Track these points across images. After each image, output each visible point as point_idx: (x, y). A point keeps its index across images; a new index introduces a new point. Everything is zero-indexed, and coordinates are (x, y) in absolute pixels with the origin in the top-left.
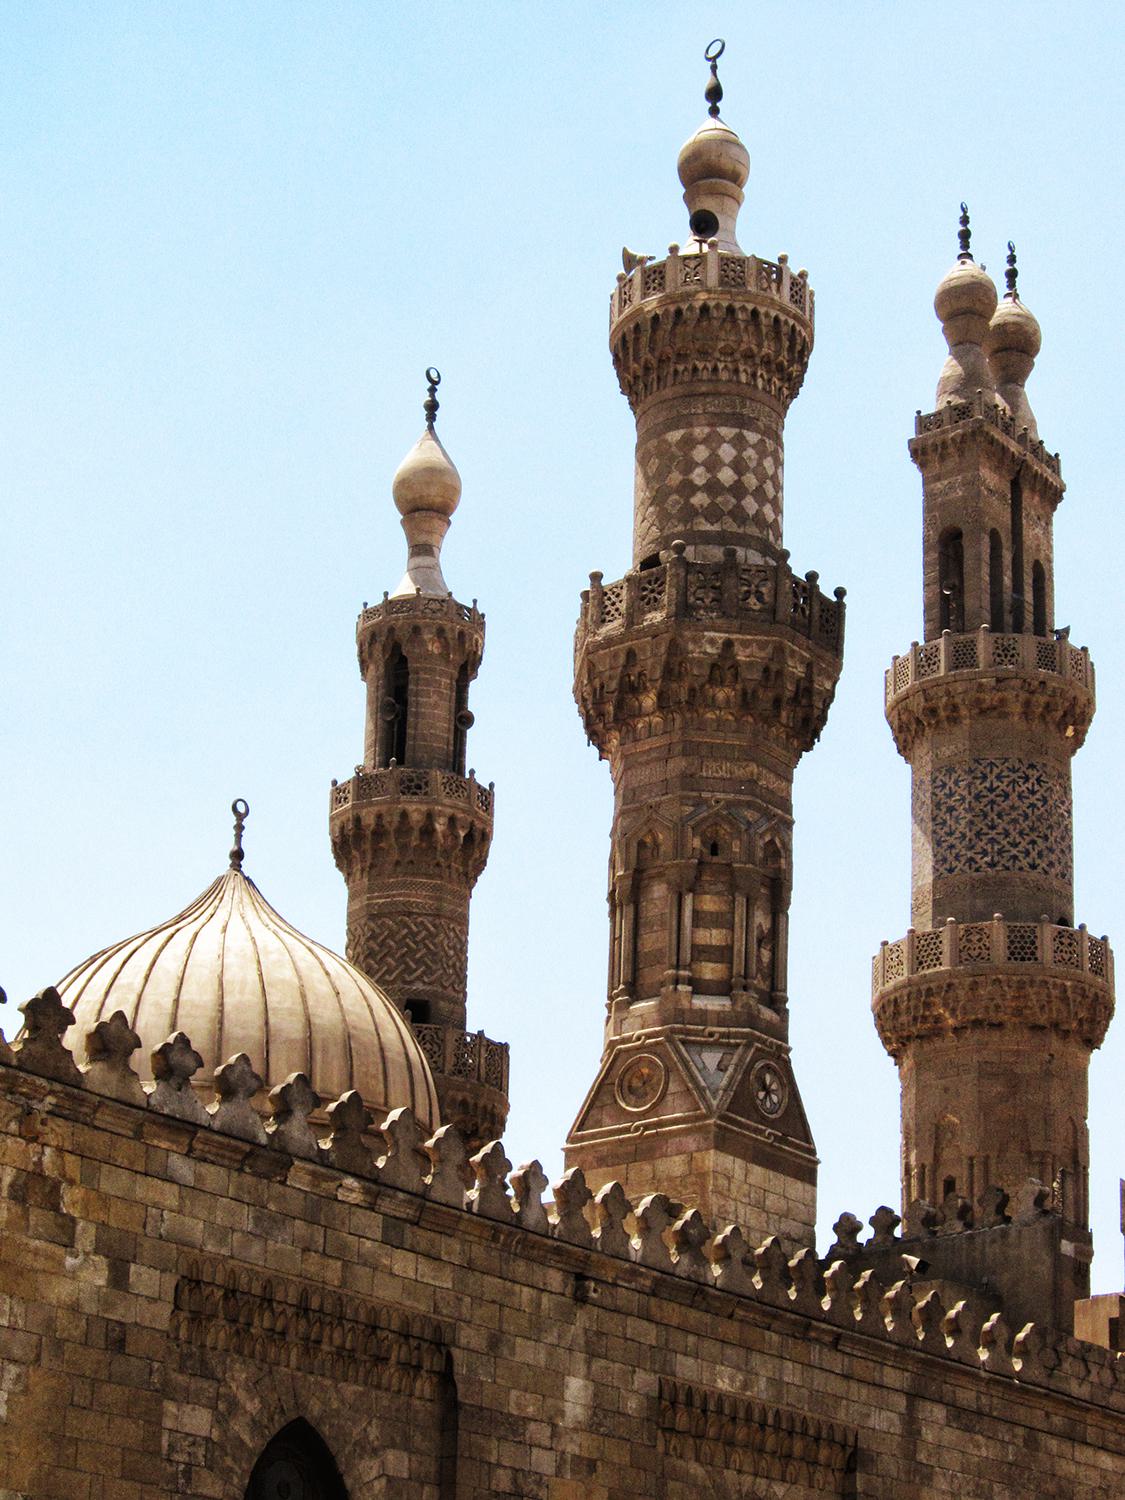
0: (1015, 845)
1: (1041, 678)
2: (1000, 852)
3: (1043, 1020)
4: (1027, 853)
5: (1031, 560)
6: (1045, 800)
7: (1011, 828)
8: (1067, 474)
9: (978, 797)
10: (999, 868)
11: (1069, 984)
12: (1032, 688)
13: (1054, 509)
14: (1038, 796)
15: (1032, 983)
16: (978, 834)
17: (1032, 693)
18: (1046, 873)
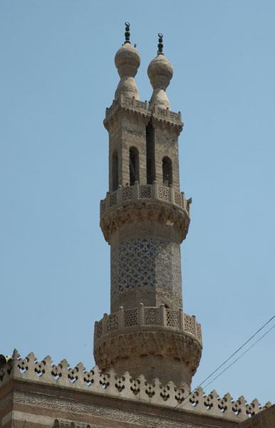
0: (136, 276)
1: (143, 202)
2: (131, 280)
3: (144, 351)
4: (143, 278)
5: (161, 157)
6: (151, 254)
7: (134, 269)
8: (184, 120)
9: (122, 259)
10: (130, 287)
11: (154, 333)
12: (139, 207)
13: (179, 135)
14: (148, 253)
15: (136, 334)
16: (122, 275)
17: (140, 209)
18: (152, 285)
